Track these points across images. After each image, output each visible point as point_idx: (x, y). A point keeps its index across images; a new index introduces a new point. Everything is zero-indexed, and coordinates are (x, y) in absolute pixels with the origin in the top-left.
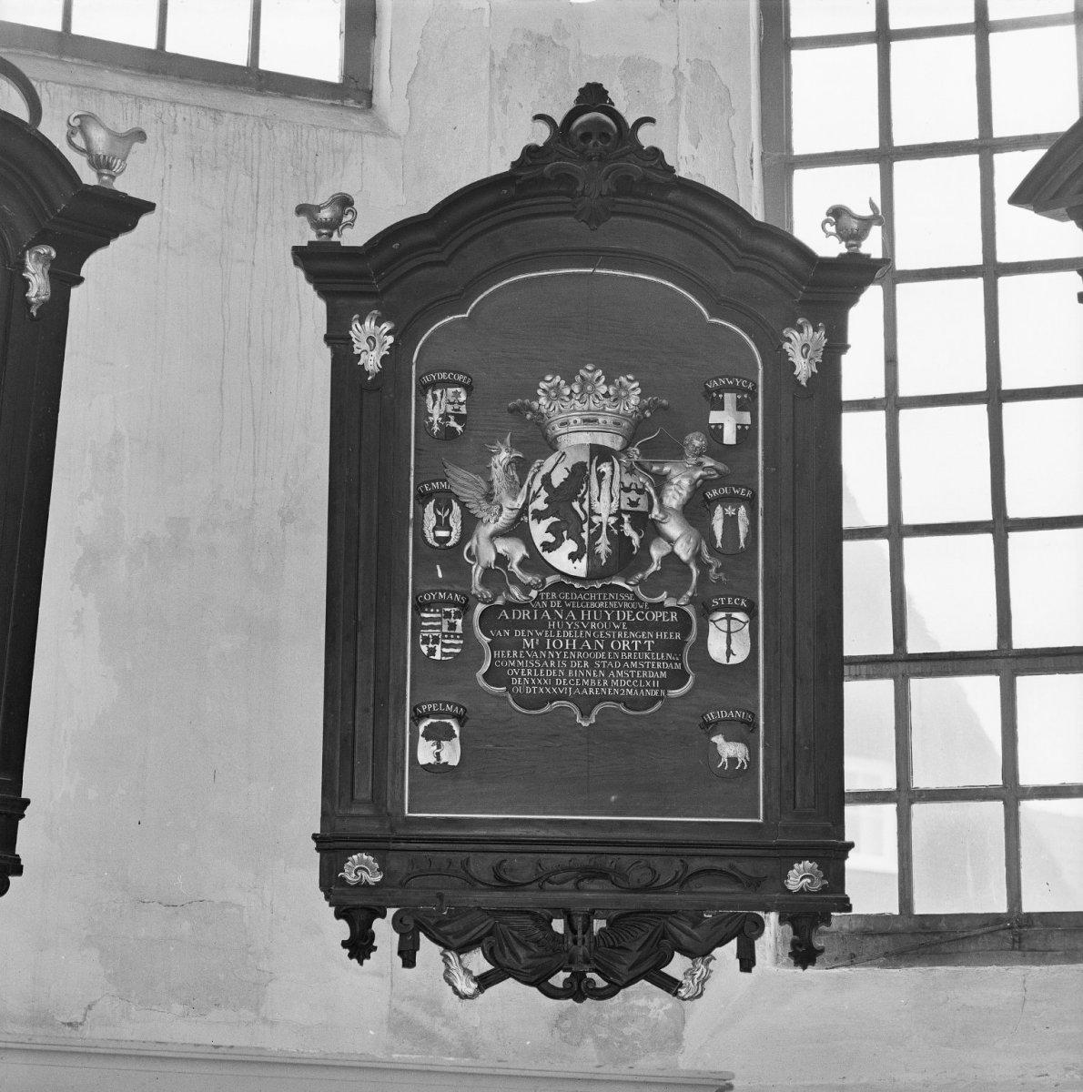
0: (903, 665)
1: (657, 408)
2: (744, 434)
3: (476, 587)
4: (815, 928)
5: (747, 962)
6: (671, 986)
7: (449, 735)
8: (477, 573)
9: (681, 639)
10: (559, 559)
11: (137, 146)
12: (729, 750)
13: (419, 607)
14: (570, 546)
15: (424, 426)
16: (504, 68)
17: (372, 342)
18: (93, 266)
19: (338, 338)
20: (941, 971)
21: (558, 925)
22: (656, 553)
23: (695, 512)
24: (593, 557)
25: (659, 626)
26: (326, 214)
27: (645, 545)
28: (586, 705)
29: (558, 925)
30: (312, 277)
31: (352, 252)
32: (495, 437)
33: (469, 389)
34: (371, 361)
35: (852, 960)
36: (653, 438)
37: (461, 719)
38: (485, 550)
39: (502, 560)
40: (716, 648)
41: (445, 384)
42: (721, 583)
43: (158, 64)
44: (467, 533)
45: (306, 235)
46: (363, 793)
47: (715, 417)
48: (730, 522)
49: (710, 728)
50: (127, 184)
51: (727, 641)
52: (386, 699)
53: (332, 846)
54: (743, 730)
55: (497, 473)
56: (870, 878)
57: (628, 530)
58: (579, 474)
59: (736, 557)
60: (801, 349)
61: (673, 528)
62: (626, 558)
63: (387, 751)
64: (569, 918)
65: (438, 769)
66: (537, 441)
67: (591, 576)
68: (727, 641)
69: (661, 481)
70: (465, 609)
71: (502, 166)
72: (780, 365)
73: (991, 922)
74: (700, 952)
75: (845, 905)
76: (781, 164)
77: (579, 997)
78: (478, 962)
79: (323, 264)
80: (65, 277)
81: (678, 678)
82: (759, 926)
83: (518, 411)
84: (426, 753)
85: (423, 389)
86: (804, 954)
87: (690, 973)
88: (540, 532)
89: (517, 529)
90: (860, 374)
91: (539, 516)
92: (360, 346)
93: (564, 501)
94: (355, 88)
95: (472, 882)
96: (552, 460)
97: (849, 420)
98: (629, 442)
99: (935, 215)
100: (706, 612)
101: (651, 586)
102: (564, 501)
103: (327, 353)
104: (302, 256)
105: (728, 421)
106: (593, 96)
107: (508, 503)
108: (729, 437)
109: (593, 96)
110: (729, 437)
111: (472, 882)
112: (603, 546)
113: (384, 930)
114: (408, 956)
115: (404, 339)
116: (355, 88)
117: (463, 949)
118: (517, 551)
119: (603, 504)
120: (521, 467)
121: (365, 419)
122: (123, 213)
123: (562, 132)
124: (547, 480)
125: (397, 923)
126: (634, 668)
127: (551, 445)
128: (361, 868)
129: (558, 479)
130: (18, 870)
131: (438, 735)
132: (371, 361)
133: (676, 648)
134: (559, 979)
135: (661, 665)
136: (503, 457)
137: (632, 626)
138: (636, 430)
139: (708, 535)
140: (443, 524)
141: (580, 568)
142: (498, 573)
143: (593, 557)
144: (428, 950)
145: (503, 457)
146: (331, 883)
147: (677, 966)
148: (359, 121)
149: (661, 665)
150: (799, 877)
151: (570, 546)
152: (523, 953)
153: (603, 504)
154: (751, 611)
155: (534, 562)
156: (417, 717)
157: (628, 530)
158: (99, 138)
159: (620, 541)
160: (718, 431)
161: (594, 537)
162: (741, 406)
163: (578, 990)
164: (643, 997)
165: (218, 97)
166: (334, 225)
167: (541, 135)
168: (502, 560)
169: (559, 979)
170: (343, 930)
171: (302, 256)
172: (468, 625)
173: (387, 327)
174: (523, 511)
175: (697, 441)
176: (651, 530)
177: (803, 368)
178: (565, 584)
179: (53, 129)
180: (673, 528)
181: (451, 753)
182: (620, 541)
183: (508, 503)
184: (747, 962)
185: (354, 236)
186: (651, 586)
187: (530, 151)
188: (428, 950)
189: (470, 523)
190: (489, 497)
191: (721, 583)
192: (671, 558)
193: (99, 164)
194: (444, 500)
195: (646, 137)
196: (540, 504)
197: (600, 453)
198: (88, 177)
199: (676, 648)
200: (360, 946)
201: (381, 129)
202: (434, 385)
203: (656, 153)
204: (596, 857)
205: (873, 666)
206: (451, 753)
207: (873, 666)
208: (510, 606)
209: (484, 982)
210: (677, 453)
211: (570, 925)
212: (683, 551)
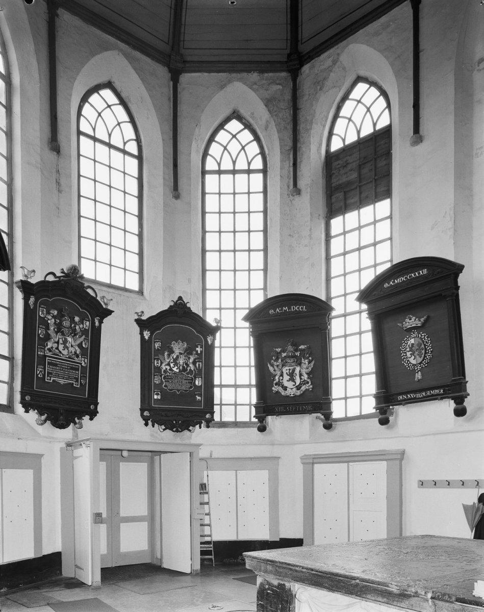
0: (221, 386)
1: (189, 347)
2: (201, 352)
3: (163, 373)
4: (209, 423)
5: (200, 427)
6: (190, 431)
7: (159, 394)
8: (163, 370)
9: (192, 381)
10: (175, 369)
11: (111, 302)
12: (198, 398)
13: (154, 375)
14: (176, 367)
15: (155, 348)
16: (165, 291)
17: (147, 335)
18: (105, 320)
19: (141, 334)
20: (226, 429)
21: (174, 422)
22: (188, 369)
23: (194, 363)
24: (180, 369)
25: (189, 380)
26: (140, 314)
27: (187, 367)
28: (178, 391)
29: (174, 422)
30: (137, 323)
31: (144, 321)
32: (165, 350)
33: (161, 342)
34: (147, 337)
35: (214, 427)
36: (189, 351)
37: (161, 392)
38: (164, 367)
39: (166, 369)
40: (197, 383)
41: (158, 342)
42: (198, 374)
43: (110, 286)
44: (161, 365)
45: (137, 317)
46: (146, 403)
47: (197, 349)
48: (199, 365)
49: (196, 395)
50: (110, 308)
51: (198, 382)
52: (150, 390)
53: (142, 410)
54: (200, 395)
55: (166, 356)
56: (217, 418)
57: (185, 365)
58: (177, 357)
59: (200, 370)
60: (209, 339)
61: (191, 365)
62: (184, 370)
63: (150, 397)
64: (176, 421)
65: (157, 399)
66: (171, 352)
67: (179, 372)
68: (198, 382)
69: (189, 358)
70: (161, 376)
71: (166, 308)
72: (206, 341)
73: (233, 423)
74: (194, 426)
75: (214, 420)
76: (204, 309)
77: (177, 432)
78: (163, 427)
79: (139, 322)
80: (101, 322)
81: (191, 387)
82: (202, 423)
83: (169, 347)
84: (156, 397)
85: (154, 342)
86: (208, 427)
87: (192, 429)
88: (172, 365)
89: (169, 364)
90: (217, 343)
91: (172, 363)
92: (145, 335)
93: (175, 360)
94: (141, 292)
95: (162, 416)
96: (173, 354)
97: (216, 349)
98: (185, 352)
99: (227, 320)
100: (195, 378)
101: (188, 374)
102: (175, 360)
103: (139, 336)
104: (137, 321)
105: (199, 349)
106: (180, 298)
107: (167, 360)
108: (199, 352)
109: (180, 298)
110: (199, 352)
111: (162, 416)
112: (181, 368)
113: (150, 422)
114: (153, 426)
115: (152, 334)
116: (141, 292)
117: (161, 425)
118: (168, 368)
119: (181, 361)
120: (169, 355)
121: (145, 346)
122: (109, 312)
123: (176, 303)
124: (173, 357)
125: (152, 421)
126: (185, 386)
127: (173, 352)
128: (146, 413)
129: (175, 357)
130: (93, 414)
131: (157, 394)
132: (147, 337)
133: (191, 383)
134: (174, 429)
135: (189, 385)
136: (166, 353)
137: (185, 379)
138: (186, 350)
139: (196, 366)
140: (158, 363)
141: (178, 371)
142: (165, 371)
143: (180, 369)
144: (156, 425)
145: (166, 353)
146: (142, 415)
147: (191, 428)
148: (141, 297)
149: (189, 385)
150: (208, 416)
151: (176, 367)
152: (170, 426)
153: (181, 361)
154: (202, 378)
155: (171, 369)
156: (154, 392)
157: (185, 365)
158: (105, 301)
159: (183, 367)
160: (198, 351)
161: (180, 366)
162: (201, 348)
163: (177, 431)
164: (186, 432)
165: (120, 292)
166: (141, 316)
167: (172, 304)
168: (166, 369)
169: (174, 429)
170: (144, 422)
171: (137, 321)
172: (161, 378)
173: (149, 332)
174: (169, 362)
175: (194, 352)
176: (188, 365)
177: (210, 342)
178: (175, 373)
179: (98, 298)
180: (191, 365)
181: (159, 397)
182: (183, 367)
183: (167, 360)
184: (200, 427)
185: (144, 318)
186: (188, 374)
187: (171, 306)
188: (156, 425)
189: (162, 363)
190: (164, 359)
191: (198, 374)
192: (190, 370)
193: (106, 304)
194: (158, 359)
195: (188, 305)
196: (172, 361)
197: (181, 354)
198: (104, 306)
199: (191, 383)
200: (146, 424)
201: (145, 299)
202: (156, 342)
203: (189, 308)
204: (180, 412)
205: (218, 386)
206: (159, 397)
207: (218, 386)
208: (167, 376)
209: (164, 430)
210: (192, 354)
211: (176, 422)
212: (192, 369)
